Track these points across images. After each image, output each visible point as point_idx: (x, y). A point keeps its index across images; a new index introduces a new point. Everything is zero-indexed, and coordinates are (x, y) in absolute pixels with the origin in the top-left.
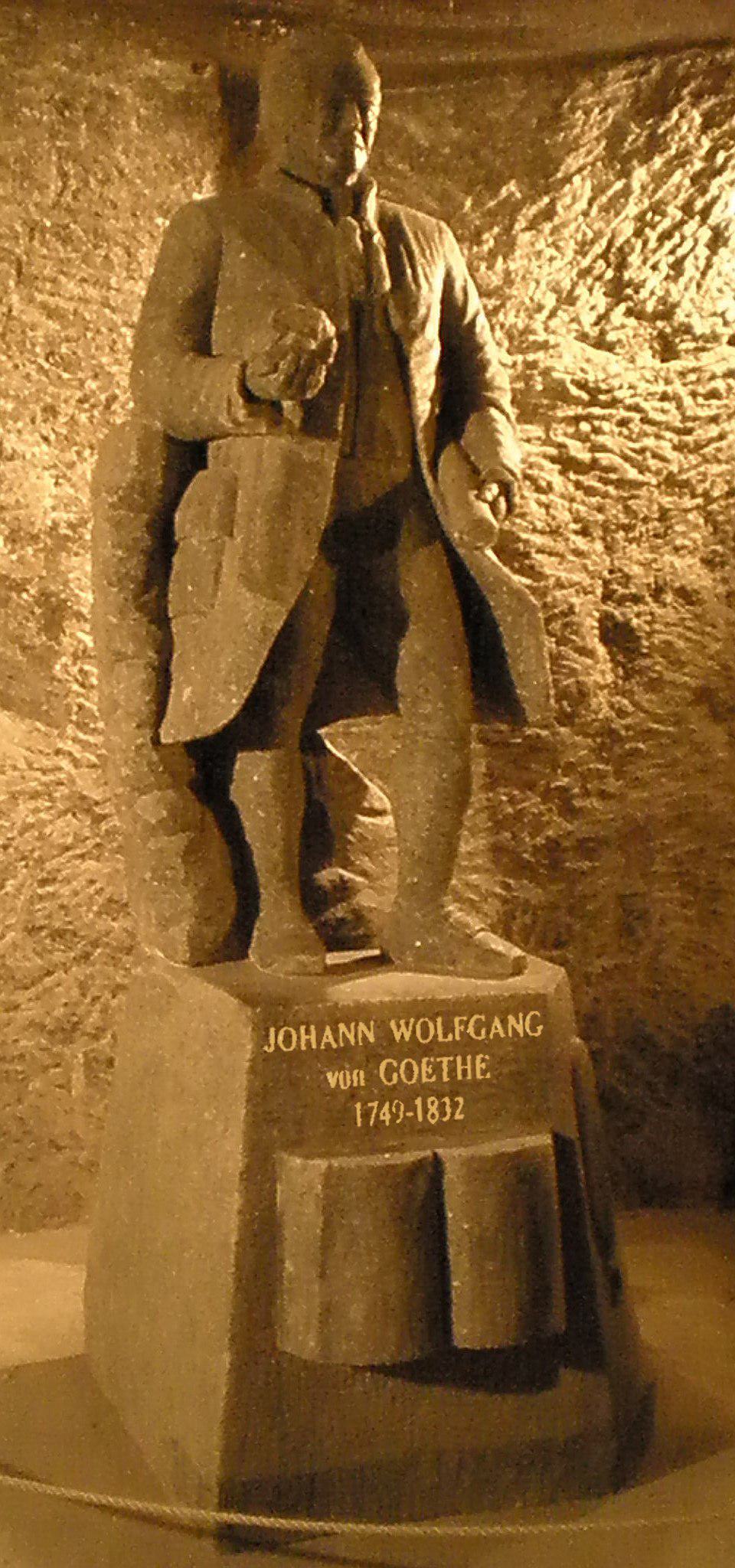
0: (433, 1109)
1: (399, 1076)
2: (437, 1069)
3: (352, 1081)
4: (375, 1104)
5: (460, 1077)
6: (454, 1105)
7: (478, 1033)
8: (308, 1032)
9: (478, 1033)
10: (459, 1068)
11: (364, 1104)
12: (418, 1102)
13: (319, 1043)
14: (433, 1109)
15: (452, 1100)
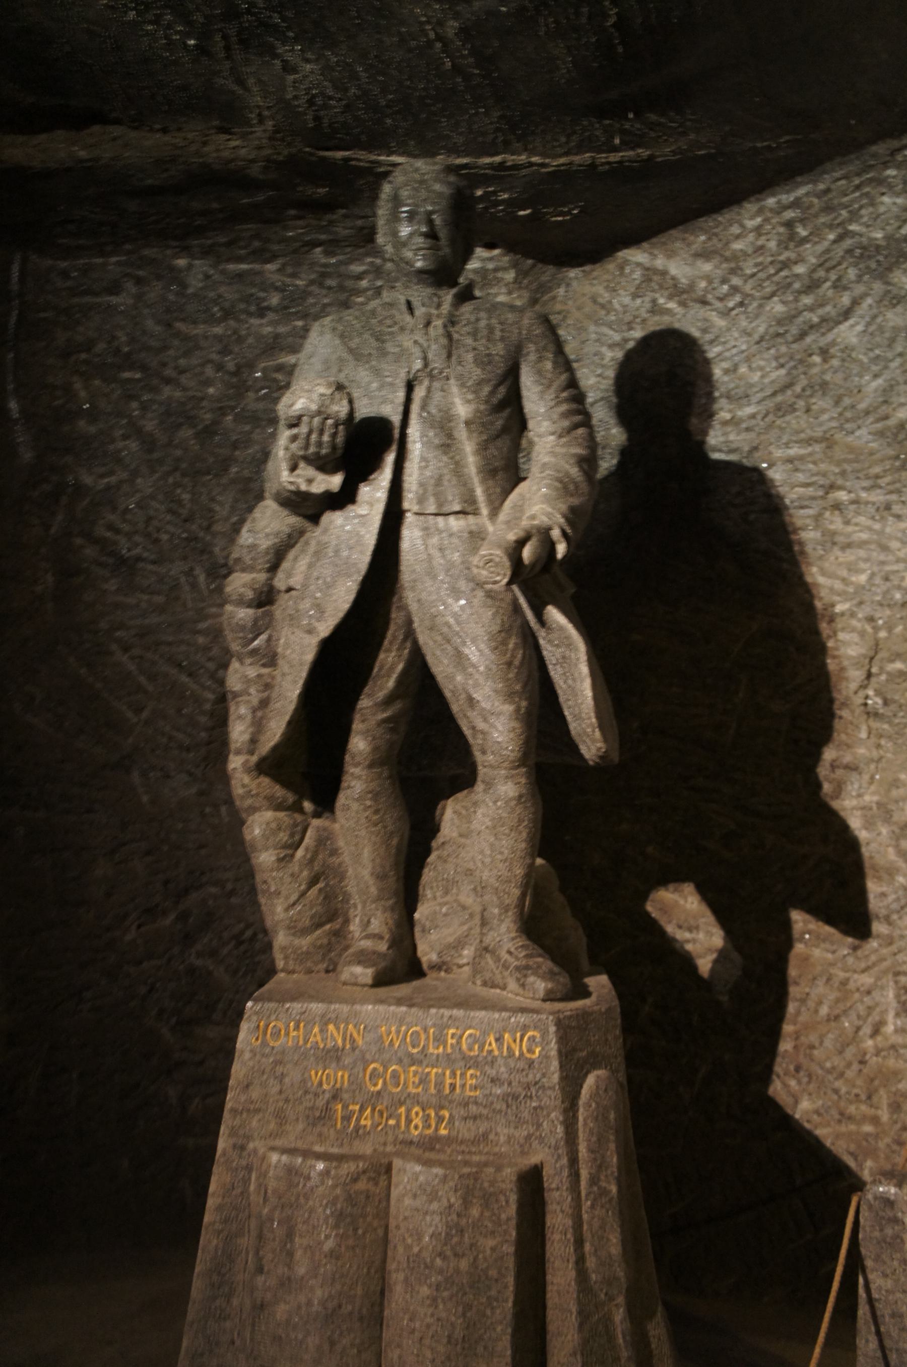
0: (417, 1121)
1: (385, 1083)
2: (424, 1080)
3: (336, 1082)
4: (357, 1107)
5: (447, 1091)
6: (440, 1119)
7: (471, 1049)
8: (297, 1028)
9: (471, 1049)
10: (448, 1081)
11: (345, 1107)
12: (402, 1110)
13: (306, 1041)
14: (417, 1121)
15: (436, 1114)
